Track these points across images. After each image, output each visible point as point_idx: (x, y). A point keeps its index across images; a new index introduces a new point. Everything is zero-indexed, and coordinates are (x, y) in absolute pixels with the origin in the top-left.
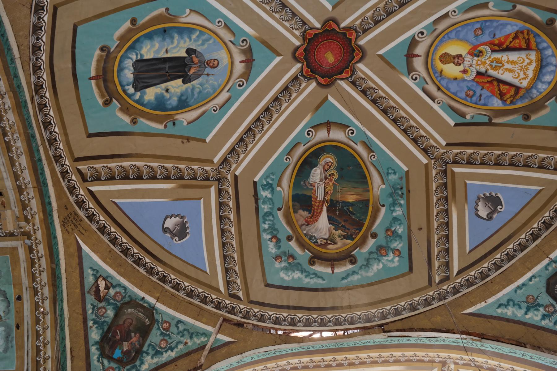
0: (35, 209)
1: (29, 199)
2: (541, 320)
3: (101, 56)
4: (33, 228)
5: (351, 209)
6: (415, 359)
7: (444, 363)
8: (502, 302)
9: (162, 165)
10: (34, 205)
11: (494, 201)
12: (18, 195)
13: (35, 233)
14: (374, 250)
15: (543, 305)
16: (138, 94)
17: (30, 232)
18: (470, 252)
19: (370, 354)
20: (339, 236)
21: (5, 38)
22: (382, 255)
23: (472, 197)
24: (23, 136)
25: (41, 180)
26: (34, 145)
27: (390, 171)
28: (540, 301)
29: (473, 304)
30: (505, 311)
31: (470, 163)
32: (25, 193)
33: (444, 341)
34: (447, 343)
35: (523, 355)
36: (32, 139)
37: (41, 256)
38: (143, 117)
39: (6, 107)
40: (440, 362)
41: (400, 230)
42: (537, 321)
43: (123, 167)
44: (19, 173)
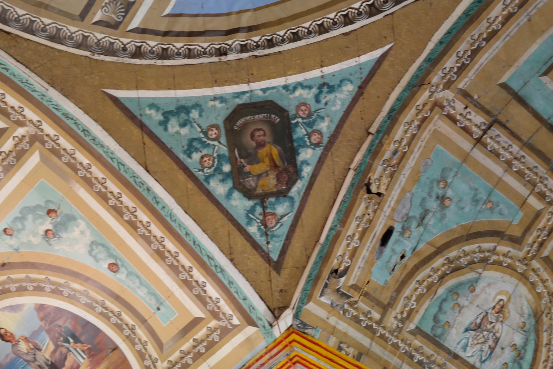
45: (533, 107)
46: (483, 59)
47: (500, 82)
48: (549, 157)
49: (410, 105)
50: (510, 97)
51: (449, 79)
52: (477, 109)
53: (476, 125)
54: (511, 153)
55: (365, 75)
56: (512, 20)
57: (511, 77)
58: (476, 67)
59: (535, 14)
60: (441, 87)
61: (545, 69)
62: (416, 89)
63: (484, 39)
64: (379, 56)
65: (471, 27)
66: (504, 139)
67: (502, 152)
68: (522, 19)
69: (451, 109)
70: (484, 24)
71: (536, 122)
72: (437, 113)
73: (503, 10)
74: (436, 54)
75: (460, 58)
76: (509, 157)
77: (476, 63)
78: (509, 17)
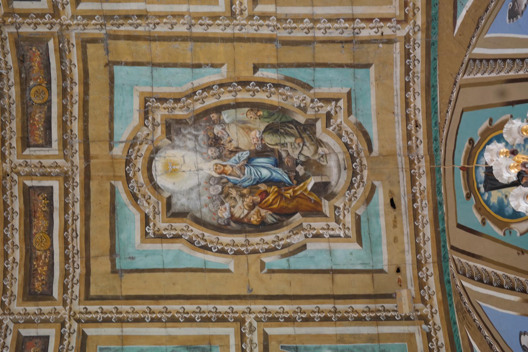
0: (433, 288)
1: (427, 276)
3: (468, 148)
4: (431, 311)
9: (506, 274)
10: (433, 283)
12: (416, 271)
13: (433, 317)
16: (487, 195)
17: (427, 316)
21: (435, 102)
24: (431, 202)
25: (443, 254)
26: (440, 213)
32: (424, 269)
36: (439, 206)
37: (441, 345)
38: (490, 220)
39: (421, 171)
43: (477, 269)
44: (422, 245)
45: (333, 69)
46: (398, 71)
47: (373, 65)
48: (286, 47)
49: (425, 7)
50: (356, 62)
51: (410, 43)
52: (372, 39)
53: (364, 28)
54: (319, 29)
55: (459, 4)
56: (404, 105)
57: (368, 74)
58: (398, 63)
59: (394, 119)
60: (411, 34)
61: (353, 95)
62: (430, 20)
63: (409, 81)
64: (457, 21)
65: (424, 82)
66: (335, 34)
67: (329, 25)
68: (399, 109)
69: (391, 25)
70: (418, 89)
71: (321, 61)
72: (400, 16)
73: (415, 106)
74: (432, 51)
75: (415, 60)
76: (319, 25)
77: (400, 65)
78: (407, 104)
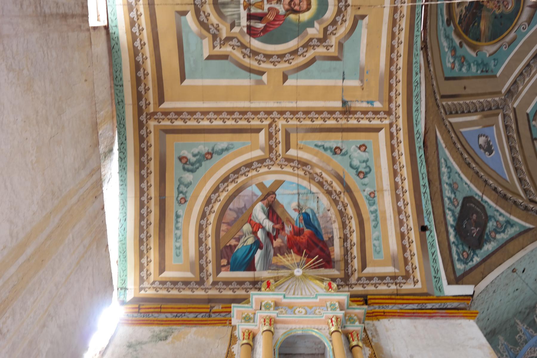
2: (447, 197)
5: (476, 24)
6: (393, 81)
7: (389, 113)
8: (448, 162)
11: (489, 149)
14: (454, 45)
15: (455, 196)
18: (461, 132)
19: (404, 31)
20: (462, 11)
22: (451, 51)
23: (486, 131)
27: (496, 61)
28: (457, 193)
29: (442, 136)
30: (444, 165)
31: (506, 127)
33: (417, 110)
34: (414, 114)
35: (424, 186)
40: (390, 109)
41: (464, 69)
42: (445, 193)
